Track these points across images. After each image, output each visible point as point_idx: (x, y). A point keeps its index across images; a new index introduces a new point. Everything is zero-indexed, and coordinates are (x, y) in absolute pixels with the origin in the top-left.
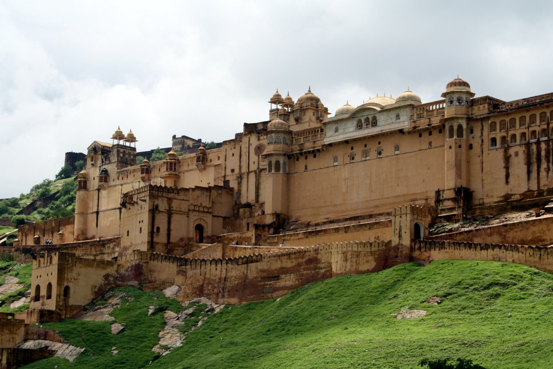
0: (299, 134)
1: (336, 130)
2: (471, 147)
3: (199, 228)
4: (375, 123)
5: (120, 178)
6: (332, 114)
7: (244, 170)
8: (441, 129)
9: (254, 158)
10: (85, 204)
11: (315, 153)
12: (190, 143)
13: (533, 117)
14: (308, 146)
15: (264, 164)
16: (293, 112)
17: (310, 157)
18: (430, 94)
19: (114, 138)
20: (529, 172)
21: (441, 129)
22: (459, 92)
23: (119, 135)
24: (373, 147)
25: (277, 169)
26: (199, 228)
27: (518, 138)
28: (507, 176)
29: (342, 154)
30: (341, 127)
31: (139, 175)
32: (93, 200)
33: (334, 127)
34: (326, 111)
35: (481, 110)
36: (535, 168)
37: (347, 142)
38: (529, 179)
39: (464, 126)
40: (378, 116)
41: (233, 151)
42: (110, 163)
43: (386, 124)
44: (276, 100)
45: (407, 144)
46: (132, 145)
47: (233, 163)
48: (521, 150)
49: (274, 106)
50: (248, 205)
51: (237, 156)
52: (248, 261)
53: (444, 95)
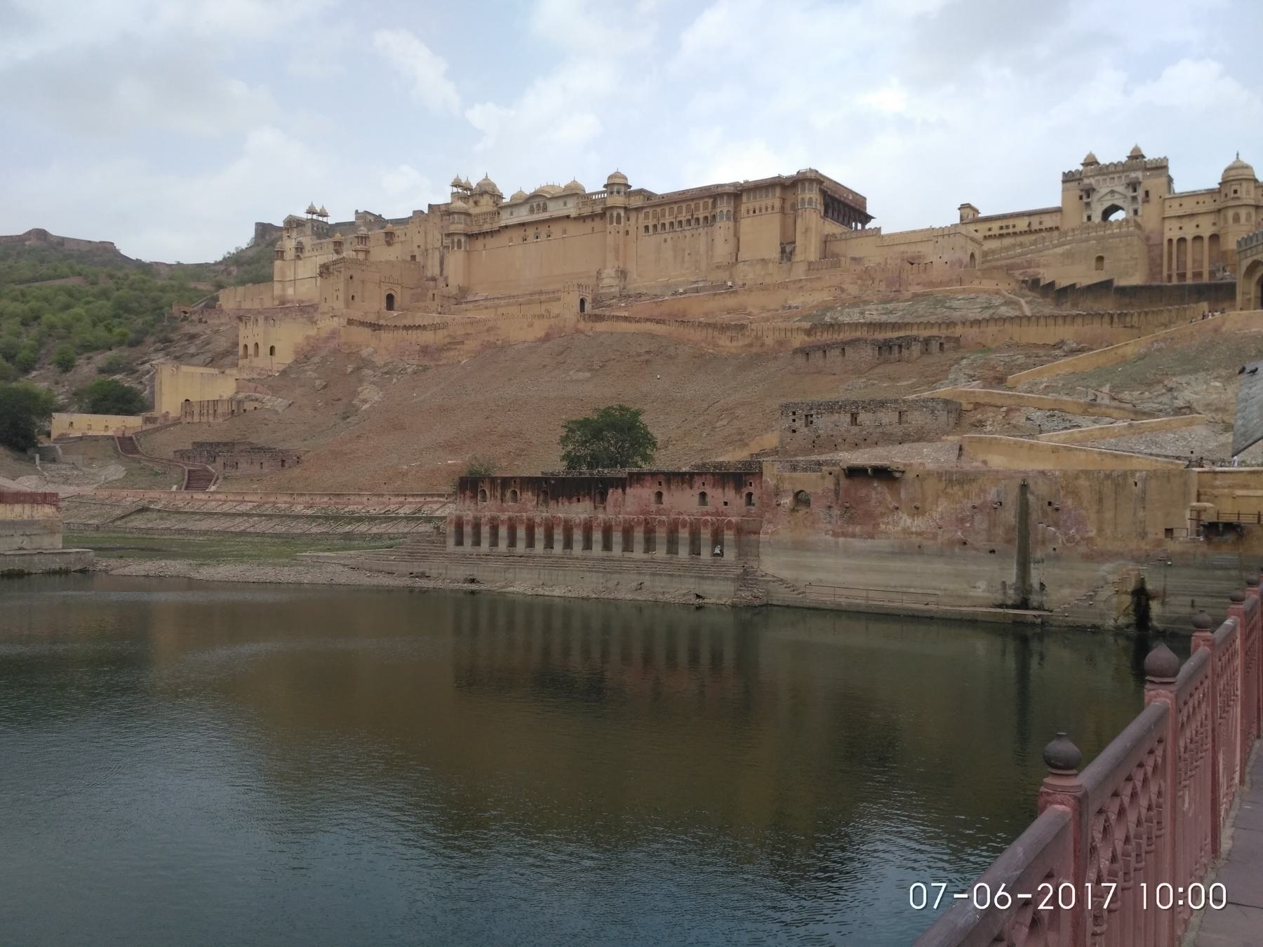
0: (476, 216)
2: (627, 233)
3: (390, 298)
4: (545, 209)
6: (507, 199)
7: (429, 246)
8: (602, 215)
10: (283, 273)
11: (492, 233)
12: (372, 219)
13: (680, 209)
14: (486, 228)
15: (447, 241)
16: (472, 196)
18: (594, 184)
19: (308, 212)
21: (602, 215)
22: (617, 184)
23: (311, 211)
24: (543, 230)
25: (459, 247)
26: (390, 298)
27: (667, 226)
29: (517, 235)
30: (516, 211)
31: (331, 246)
33: (509, 211)
34: (501, 197)
35: (636, 202)
39: (622, 214)
43: (555, 209)
44: (456, 184)
45: (573, 229)
46: (325, 219)
47: (418, 239)
49: (455, 190)
50: (434, 279)
51: (423, 234)
52: (435, 327)
53: (605, 186)
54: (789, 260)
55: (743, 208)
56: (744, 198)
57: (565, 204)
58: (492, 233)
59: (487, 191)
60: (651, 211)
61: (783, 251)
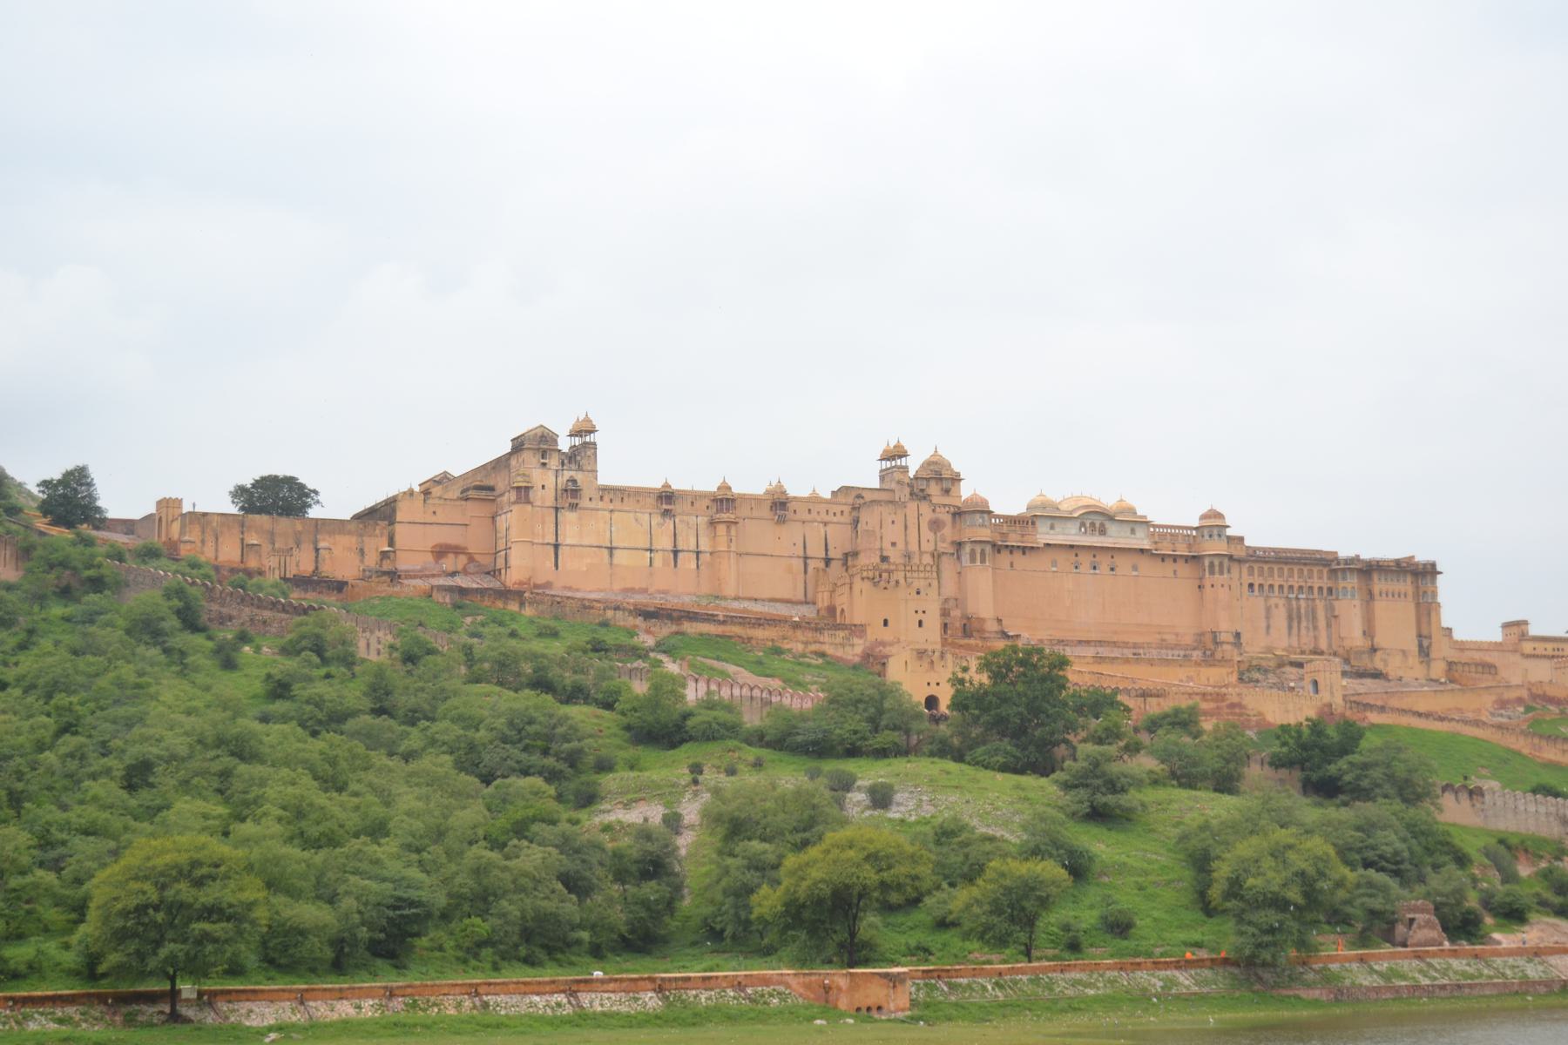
1: (1052, 527)
4: (1103, 532)
5: (606, 498)
7: (914, 547)
9: (927, 533)
11: (1024, 550)
17: (1018, 555)
20: (1290, 628)
22: (1213, 524)
24: (1104, 561)
28: (1268, 627)
29: (1064, 558)
30: (1059, 527)
32: (543, 523)
33: (1049, 522)
36: (1295, 624)
37: (1072, 547)
38: (1290, 634)
40: (1108, 525)
41: (893, 517)
42: (580, 469)
43: (1116, 537)
48: (1281, 602)
54: (1428, 655)
55: (1376, 590)
56: (1375, 576)
57: (1133, 531)
58: (1024, 550)
59: (940, 476)
60: (1256, 566)
61: (1420, 646)
